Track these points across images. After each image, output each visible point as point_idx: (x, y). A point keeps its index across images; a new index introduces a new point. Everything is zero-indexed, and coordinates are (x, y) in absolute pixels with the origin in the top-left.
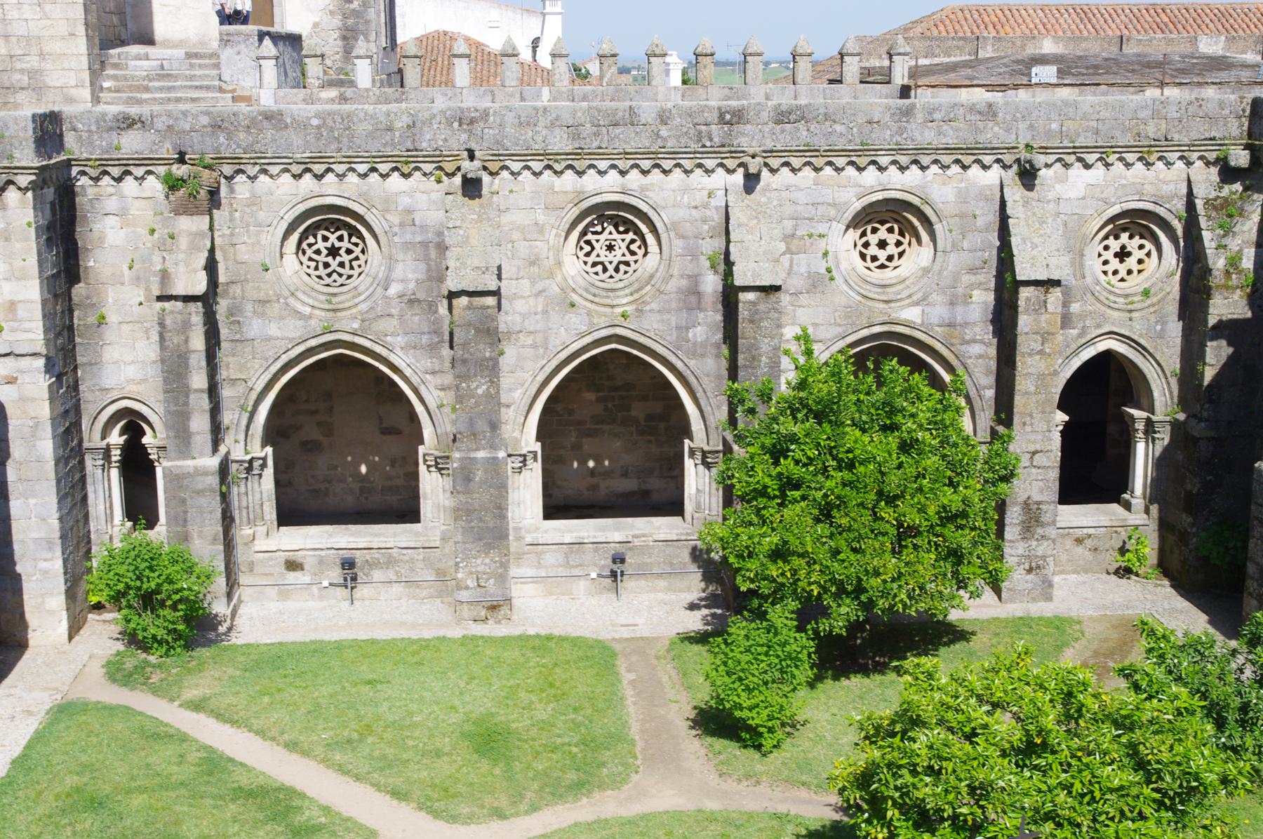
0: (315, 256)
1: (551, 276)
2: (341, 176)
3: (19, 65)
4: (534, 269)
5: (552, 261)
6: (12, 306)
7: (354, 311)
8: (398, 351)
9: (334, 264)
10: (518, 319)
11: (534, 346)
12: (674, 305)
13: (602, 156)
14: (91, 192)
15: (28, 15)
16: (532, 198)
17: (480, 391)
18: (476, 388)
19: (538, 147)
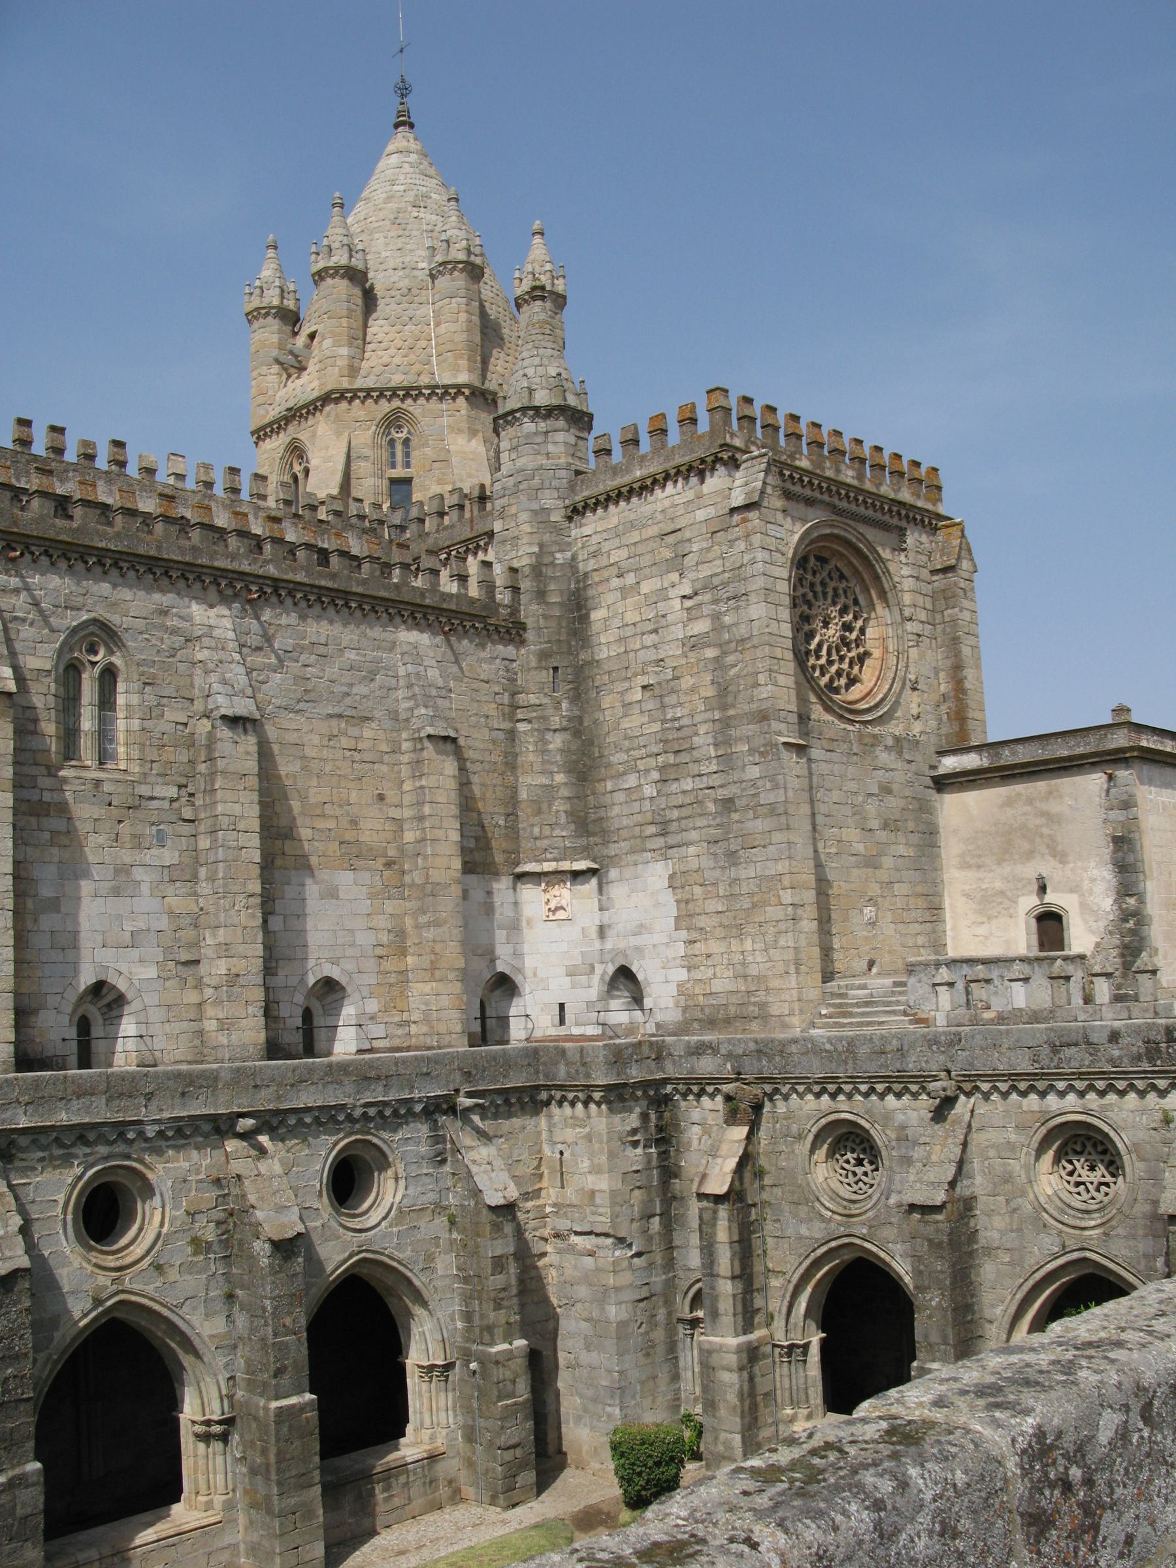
0: (845, 1165)
1: (1023, 1194)
2: (850, 1096)
3: (753, 999)
4: (1008, 1187)
5: (1024, 1179)
6: (593, 1193)
7: (864, 1217)
8: (898, 1258)
9: (859, 1170)
10: (996, 1235)
11: (1012, 1263)
12: (1141, 1232)
13: (1060, 1076)
14: (683, 1104)
15: (759, 959)
16: (1004, 1117)
17: (933, 1303)
18: (931, 1300)
19: (1002, 1068)
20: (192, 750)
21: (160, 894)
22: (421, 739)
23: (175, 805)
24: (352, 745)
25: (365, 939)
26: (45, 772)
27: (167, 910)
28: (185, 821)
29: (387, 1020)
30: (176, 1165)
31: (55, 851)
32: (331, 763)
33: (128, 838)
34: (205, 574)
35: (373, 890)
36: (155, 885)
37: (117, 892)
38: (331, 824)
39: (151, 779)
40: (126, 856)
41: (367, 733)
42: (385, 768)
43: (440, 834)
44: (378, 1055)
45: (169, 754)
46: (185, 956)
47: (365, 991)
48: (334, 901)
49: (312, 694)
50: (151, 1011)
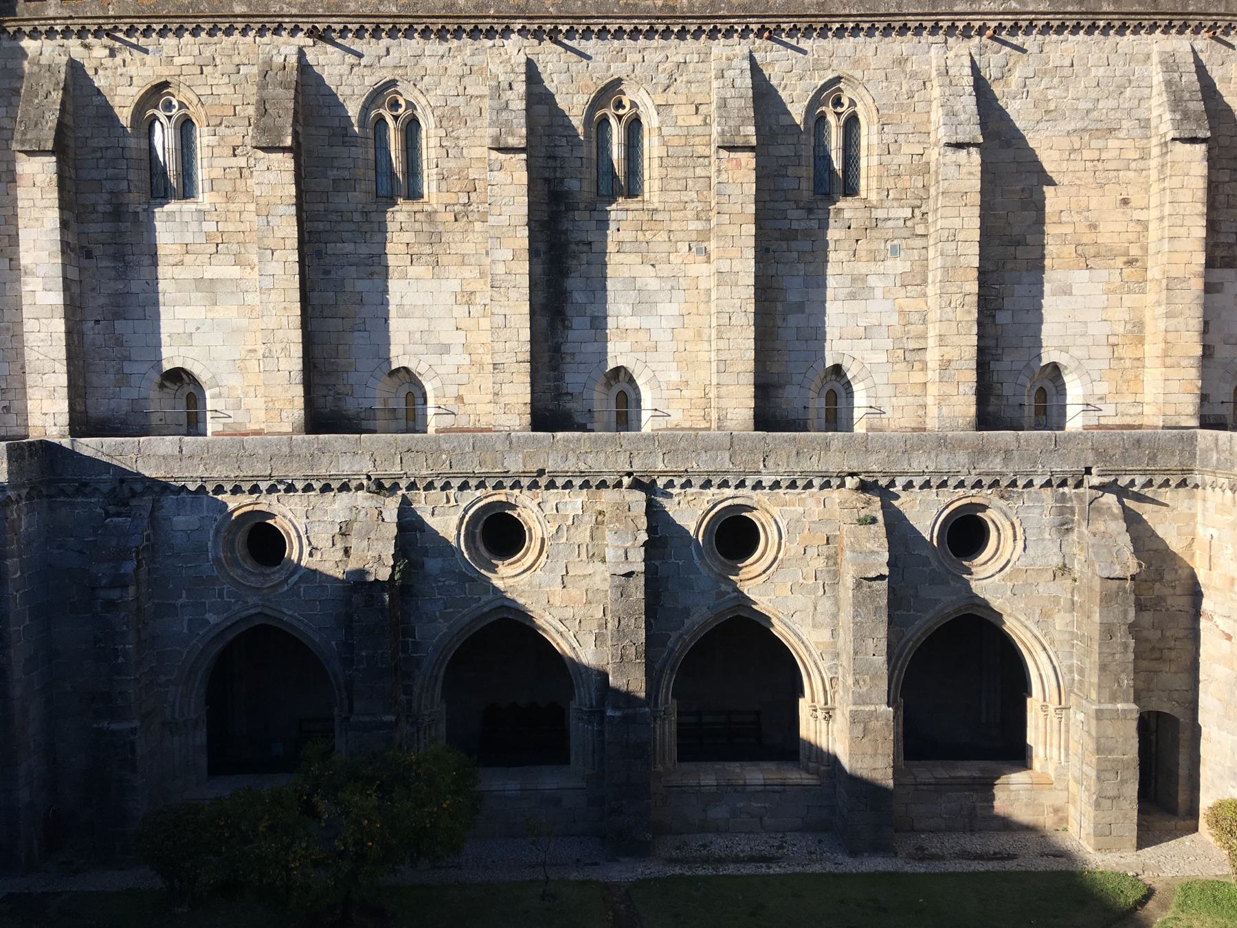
20: (927, 176)
21: (892, 297)
22: (1166, 143)
23: (909, 223)
24: (1095, 155)
25: (1098, 330)
26: (794, 206)
27: (897, 309)
28: (917, 236)
29: (1118, 400)
30: (793, 508)
31: (801, 266)
32: (1071, 175)
33: (864, 253)
34: (943, 20)
35: (1109, 286)
36: (886, 290)
37: (853, 296)
38: (1068, 229)
39: (886, 204)
40: (862, 267)
41: (1113, 143)
42: (1131, 174)
43: (1182, 232)
44: (1144, 431)
45: (905, 182)
46: (912, 345)
47: (1095, 376)
48: (1067, 297)
49: (1054, 114)
50: (880, 388)
